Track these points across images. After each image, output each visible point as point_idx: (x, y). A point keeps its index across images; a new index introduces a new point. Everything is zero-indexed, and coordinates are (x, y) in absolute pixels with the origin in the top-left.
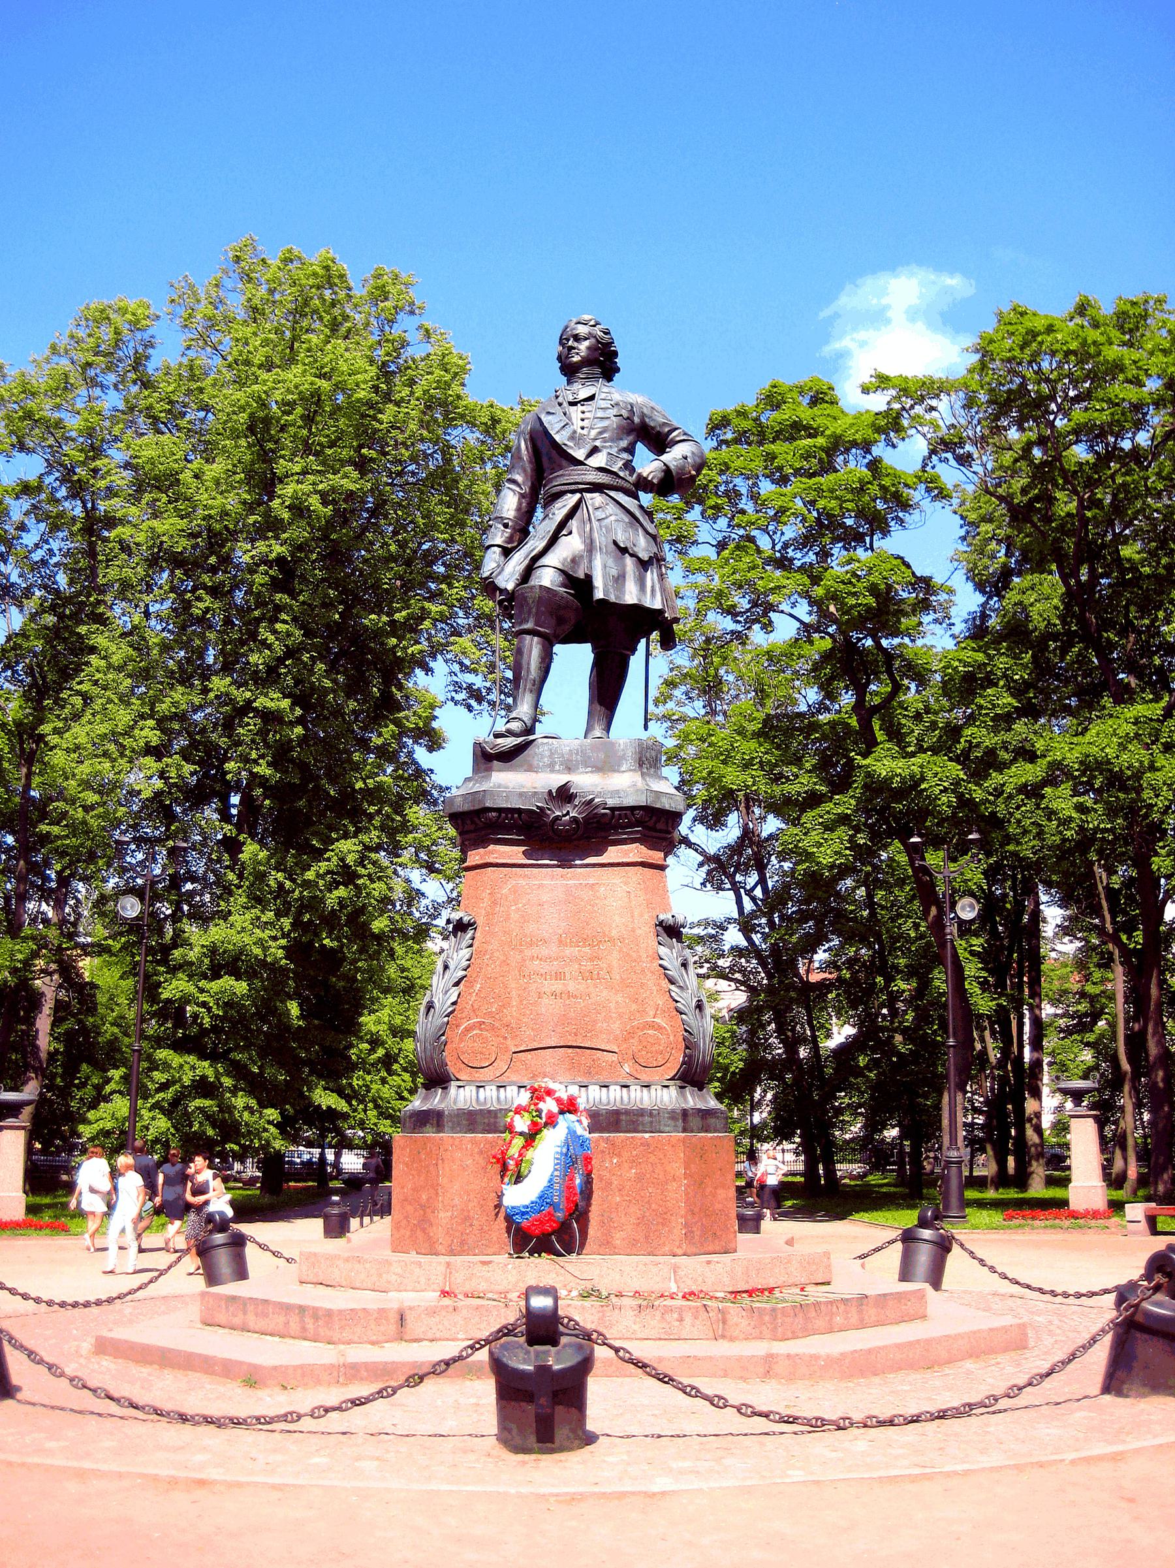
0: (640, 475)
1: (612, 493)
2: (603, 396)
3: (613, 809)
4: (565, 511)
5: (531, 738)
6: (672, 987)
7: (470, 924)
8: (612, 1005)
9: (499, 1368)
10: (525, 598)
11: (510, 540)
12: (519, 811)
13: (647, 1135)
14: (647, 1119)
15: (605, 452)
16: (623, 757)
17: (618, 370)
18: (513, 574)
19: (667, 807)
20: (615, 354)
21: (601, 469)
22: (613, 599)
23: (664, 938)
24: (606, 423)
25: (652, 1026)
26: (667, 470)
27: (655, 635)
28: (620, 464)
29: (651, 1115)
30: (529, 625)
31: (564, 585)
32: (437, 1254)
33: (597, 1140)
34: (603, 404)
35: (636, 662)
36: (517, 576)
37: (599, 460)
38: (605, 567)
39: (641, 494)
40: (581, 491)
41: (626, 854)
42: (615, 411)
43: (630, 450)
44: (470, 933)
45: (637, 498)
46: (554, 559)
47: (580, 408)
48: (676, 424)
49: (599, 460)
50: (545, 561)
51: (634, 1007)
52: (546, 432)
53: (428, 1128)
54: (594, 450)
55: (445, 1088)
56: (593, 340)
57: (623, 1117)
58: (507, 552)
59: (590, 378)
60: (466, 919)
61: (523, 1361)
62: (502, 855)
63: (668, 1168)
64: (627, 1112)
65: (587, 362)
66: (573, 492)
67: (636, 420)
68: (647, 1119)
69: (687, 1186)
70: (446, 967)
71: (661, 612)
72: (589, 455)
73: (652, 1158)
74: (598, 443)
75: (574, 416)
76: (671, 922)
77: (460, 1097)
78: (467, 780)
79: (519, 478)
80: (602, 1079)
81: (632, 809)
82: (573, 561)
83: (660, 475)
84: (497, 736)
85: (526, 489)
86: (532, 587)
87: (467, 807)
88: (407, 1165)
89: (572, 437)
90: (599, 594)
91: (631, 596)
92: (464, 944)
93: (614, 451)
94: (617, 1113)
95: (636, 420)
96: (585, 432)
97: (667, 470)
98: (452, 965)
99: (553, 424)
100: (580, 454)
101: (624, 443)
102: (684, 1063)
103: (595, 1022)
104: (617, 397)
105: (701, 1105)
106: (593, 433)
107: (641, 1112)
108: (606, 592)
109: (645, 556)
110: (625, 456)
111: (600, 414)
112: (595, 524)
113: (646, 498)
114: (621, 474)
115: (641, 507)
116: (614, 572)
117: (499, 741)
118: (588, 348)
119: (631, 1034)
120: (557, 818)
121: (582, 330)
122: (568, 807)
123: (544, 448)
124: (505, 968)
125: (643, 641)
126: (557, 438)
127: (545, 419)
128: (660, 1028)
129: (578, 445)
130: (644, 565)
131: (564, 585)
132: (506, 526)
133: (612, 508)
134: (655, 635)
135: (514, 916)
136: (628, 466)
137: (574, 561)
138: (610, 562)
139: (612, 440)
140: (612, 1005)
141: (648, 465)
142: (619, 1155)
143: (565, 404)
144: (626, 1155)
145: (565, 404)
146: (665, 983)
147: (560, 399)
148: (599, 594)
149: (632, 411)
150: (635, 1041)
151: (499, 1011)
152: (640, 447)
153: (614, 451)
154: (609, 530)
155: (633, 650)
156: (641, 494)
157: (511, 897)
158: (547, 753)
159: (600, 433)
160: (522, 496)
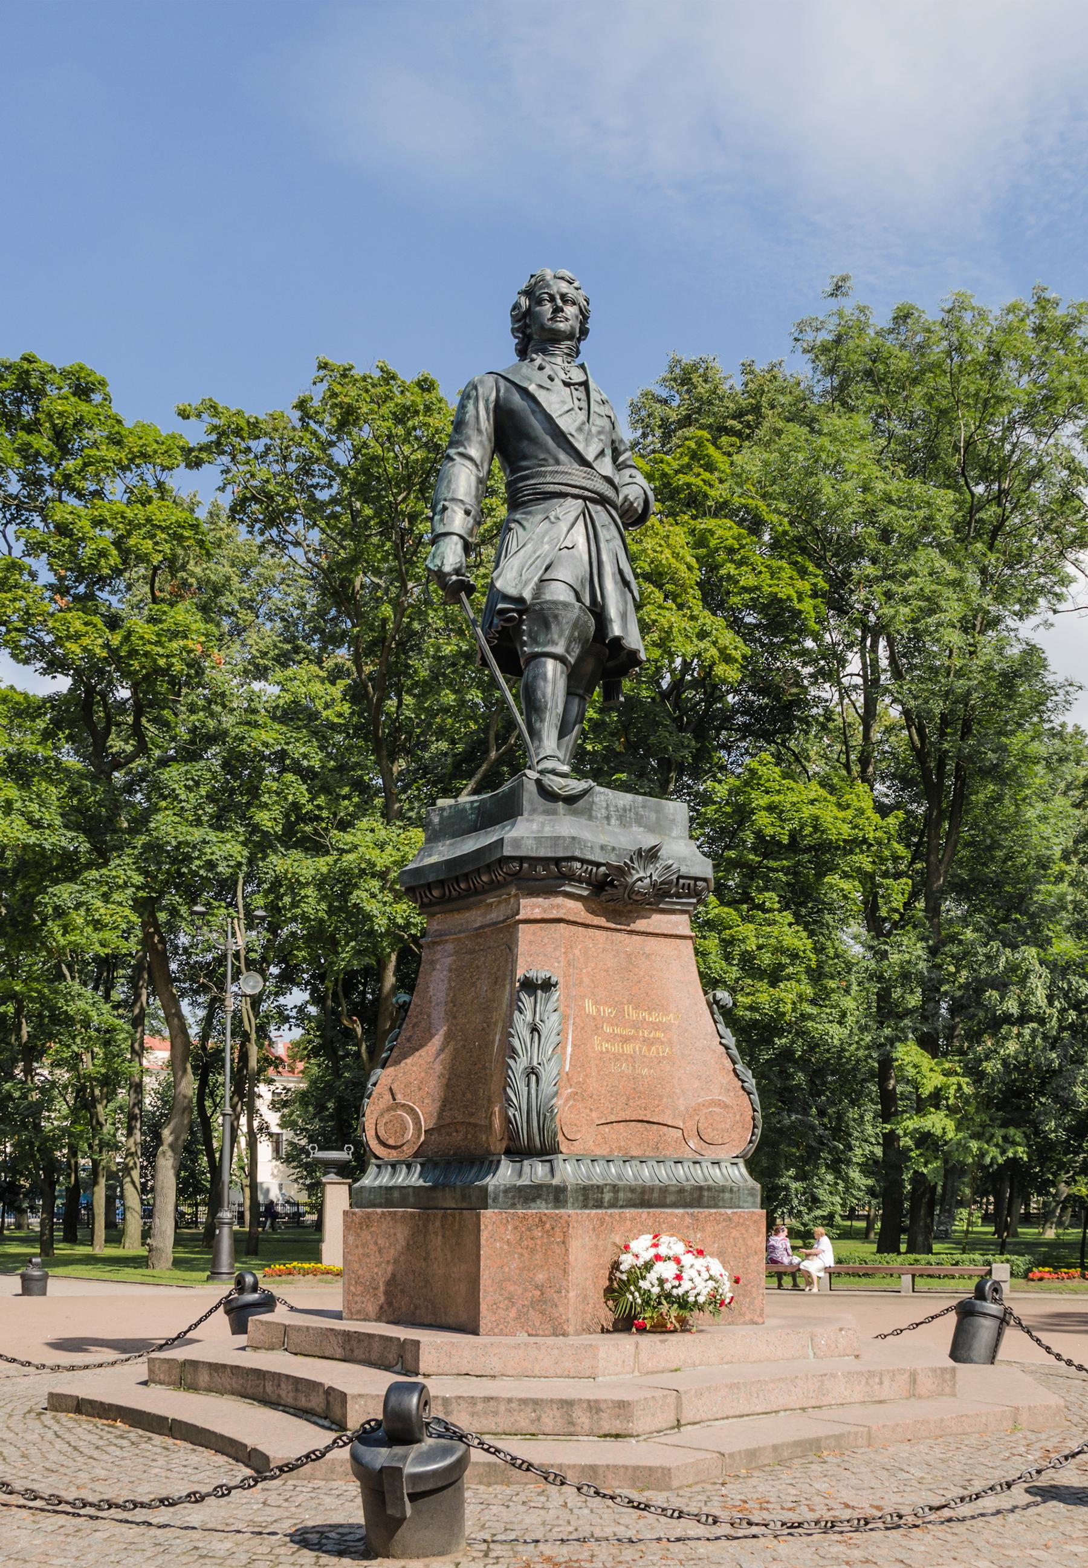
8: (676, 1081)
10: (556, 617)
13: (729, 1211)
14: (727, 1195)
29: (731, 1191)
40: (585, 498)
51: (697, 1083)
57: (706, 1193)
63: (750, 1243)
64: (709, 1188)
66: (576, 497)
68: (727, 1195)
72: (596, 458)
73: (735, 1233)
77: (568, 1173)
88: (508, 1242)
94: (701, 1188)
103: (661, 1097)
107: (723, 1189)
128: (726, 1106)
135: (586, 980)
142: (703, 1230)
144: (709, 1229)
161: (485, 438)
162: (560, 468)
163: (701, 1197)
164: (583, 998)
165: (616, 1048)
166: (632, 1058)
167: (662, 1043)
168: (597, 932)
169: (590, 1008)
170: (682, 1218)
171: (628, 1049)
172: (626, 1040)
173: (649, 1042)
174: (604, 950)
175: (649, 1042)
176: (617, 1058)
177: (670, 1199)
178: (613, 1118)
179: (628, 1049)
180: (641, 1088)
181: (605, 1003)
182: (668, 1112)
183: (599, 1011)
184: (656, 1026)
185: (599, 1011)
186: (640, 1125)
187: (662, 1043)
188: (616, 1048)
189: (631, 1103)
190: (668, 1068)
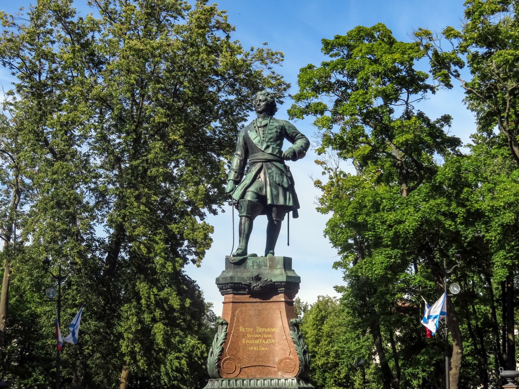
1: (274, 163)
3: (274, 282)
4: (257, 170)
5: (246, 257)
11: (237, 177)
12: (241, 283)
16: (278, 263)
19: (293, 281)
21: (270, 154)
24: (272, 135)
25: (289, 358)
26: (294, 152)
27: (291, 213)
31: (256, 198)
34: (271, 127)
35: (284, 223)
37: (270, 151)
39: (285, 161)
40: (263, 162)
41: (280, 298)
42: (275, 130)
43: (281, 145)
45: (284, 163)
46: (252, 188)
49: (270, 151)
50: (250, 189)
51: (282, 352)
52: (249, 138)
54: (268, 147)
56: (266, 101)
58: (237, 182)
62: (236, 299)
70: (217, 339)
72: (266, 148)
74: (269, 143)
78: (223, 272)
80: (272, 377)
81: (281, 282)
83: (292, 154)
84: (234, 256)
86: (245, 201)
87: (224, 282)
89: (259, 142)
92: (224, 330)
93: (274, 146)
96: (264, 139)
97: (294, 152)
98: (219, 339)
101: (278, 142)
103: (269, 357)
104: (276, 124)
105: (305, 386)
106: (267, 140)
108: (272, 200)
109: (286, 186)
111: (269, 132)
113: (287, 163)
114: (278, 155)
115: (285, 166)
116: (275, 193)
119: (281, 361)
124: (238, 339)
125: (287, 214)
126: (254, 141)
128: (291, 359)
129: (262, 145)
130: (285, 190)
132: (236, 172)
133: (274, 169)
134: (291, 213)
135: (241, 320)
136: (280, 152)
137: (261, 189)
138: (274, 189)
141: (287, 146)
145: (257, 128)
146: (293, 344)
147: (255, 125)
148: (269, 202)
150: (282, 364)
151: (236, 354)
153: (274, 146)
154: (273, 177)
155: (283, 219)
156: (285, 161)
157: (239, 314)
159: (270, 139)
160: (241, 161)
161: (242, 148)
162: (255, 154)
164: (238, 326)
165: (252, 342)
166: (258, 345)
168: (248, 304)
169: (242, 329)
171: (257, 342)
172: (257, 338)
173: (266, 339)
174: (249, 310)
176: (252, 345)
178: (249, 365)
179: (257, 342)
180: (261, 354)
181: (249, 327)
182: (271, 362)
183: (245, 330)
184: (269, 333)
185: (245, 330)
187: (271, 338)
188: (252, 342)
189: (257, 360)
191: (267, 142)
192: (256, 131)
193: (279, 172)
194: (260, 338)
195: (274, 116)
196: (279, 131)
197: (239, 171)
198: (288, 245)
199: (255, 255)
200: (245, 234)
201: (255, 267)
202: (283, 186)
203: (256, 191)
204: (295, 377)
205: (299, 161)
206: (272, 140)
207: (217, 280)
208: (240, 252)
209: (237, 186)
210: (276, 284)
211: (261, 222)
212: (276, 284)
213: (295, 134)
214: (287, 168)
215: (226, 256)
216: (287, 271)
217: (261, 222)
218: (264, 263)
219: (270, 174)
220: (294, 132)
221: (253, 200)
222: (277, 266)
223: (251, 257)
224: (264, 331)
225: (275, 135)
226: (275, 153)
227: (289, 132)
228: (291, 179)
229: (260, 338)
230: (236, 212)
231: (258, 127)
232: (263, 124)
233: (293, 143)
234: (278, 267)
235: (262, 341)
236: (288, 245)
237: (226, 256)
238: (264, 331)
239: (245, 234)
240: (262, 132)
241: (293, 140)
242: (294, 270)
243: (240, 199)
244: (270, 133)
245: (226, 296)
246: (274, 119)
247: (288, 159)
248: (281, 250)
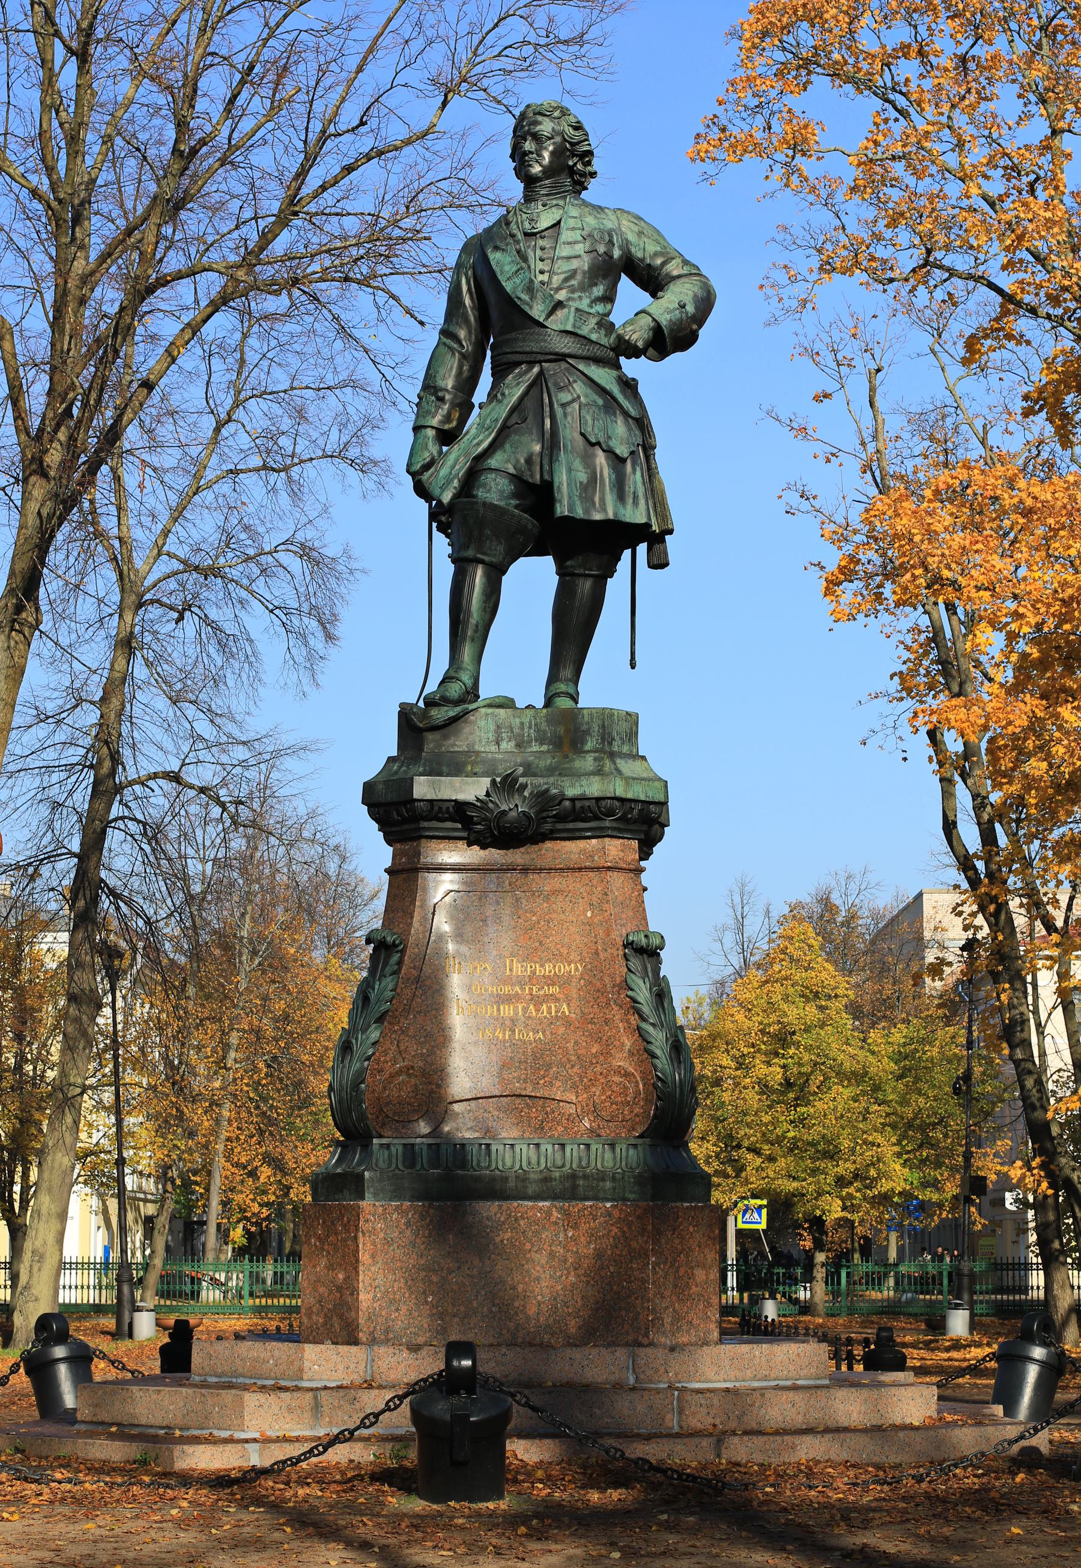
0: (620, 338)
2: (571, 223)
3: (573, 800)
4: (519, 392)
6: (644, 1025)
7: (394, 945)
8: (570, 1045)
9: (417, 1416)
11: (448, 418)
13: (608, 1205)
15: (574, 305)
16: (587, 732)
17: (593, 175)
18: (448, 481)
20: (590, 153)
22: (580, 513)
23: (635, 963)
24: (575, 264)
26: (657, 329)
27: (642, 549)
28: (593, 321)
30: (470, 553)
32: (355, 1342)
33: (550, 1208)
35: (617, 587)
36: (456, 483)
38: (570, 470)
39: (622, 359)
40: (540, 362)
43: (609, 298)
44: (396, 958)
45: (618, 367)
47: (541, 242)
48: (676, 242)
50: (493, 462)
53: (346, 1193)
55: (366, 1146)
59: (556, 192)
60: (389, 939)
61: (441, 1408)
64: (585, 1177)
65: (549, 172)
66: (531, 364)
67: (617, 253)
69: (656, 1264)
71: (648, 525)
74: (562, 295)
75: (530, 253)
76: (644, 941)
78: (391, 760)
79: (462, 334)
81: (598, 799)
82: (529, 461)
85: (468, 347)
87: (391, 797)
88: (319, 1238)
90: (562, 509)
91: (607, 508)
93: (584, 304)
94: (573, 1176)
95: (617, 253)
96: (545, 278)
97: (657, 329)
98: (372, 996)
99: (502, 261)
100: (537, 311)
101: (599, 291)
102: (655, 1115)
106: (556, 280)
109: (622, 450)
110: (600, 308)
112: (559, 411)
113: (631, 367)
114: (594, 337)
116: (582, 476)
117: (434, 712)
118: (552, 153)
120: (504, 813)
121: (546, 127)
122: (517, 799)
123: (492, 298)
125: (627, 554)
126: (508, 286)
127: (494, 257)
128: (627, 1075)
131: (515, 495)
133: (579, 388)
134: (642, 549)
138: (577, 464)
139: (583, 288)
140: (570, 1045)
142: (575, 1227)
143: (520, 236)
144: (584, 1227)
145: (520, 236)
146: (634, 1020)
148: (562, 509)
149: (611, 242)
152: (625, 284)
155: (610, 572)
158: (492, 727)
159: (566, 280)
160: (463, 356)
162: (513, 335)
163: (575, 1187)
167: (557, 1000)
170: (549, 1214)
175: (537, 1001)
177: (531, 1189)
186: (518, 1101)
187: (557, 1000)
190: (562, 1030)
191: (559, 289)
192: (518, 252)
193: (600, 402)
194: (517, 998)
195: (584, 195)
196: (602, 249)
197: (455, 396)
198: (633, 666)
199: (507, 703)
200: (469, 625)
201: (504, 745)
202: (609, 452)
203: (512, 471)
204: (641, 1136)
205: (676, 357)
206: (573, 282)
207: (369, 789)
208: (455, 690)
209: (445, 449)
210: (578, 804)
211: (532, 581)
212: (578, 804)
213: (659, 261)
214: (630, 386)
215: (402, 705)
216: (618, 761)
217: (532, 584)
218: (538, 731)
219: (564, 405)
220: (656, 254)
221: (502, 504)
222: (584, 742)
223: (490, 711)
224: (534, 972)
225: (584, 264)
226: (584, 331)
227: (640, 255)
228: (642, 424)
229: (517, 998)
230: (442, 544)
231: (526, 234)
232: (545, 221)
233: (654, 295)
234: (589, 746)
235: (525, 1010)
236: (633, 666)
237: (402, 705)
238: (534, 972)
239: (469, 625)
240: (539, 252)
241: (652, 281)
242: (643, 758)
243: (456, 496)
244: (569, 258)
245: (398, 846)
246: (586, 204)
247: (633, 352)
248: (600, 685)
